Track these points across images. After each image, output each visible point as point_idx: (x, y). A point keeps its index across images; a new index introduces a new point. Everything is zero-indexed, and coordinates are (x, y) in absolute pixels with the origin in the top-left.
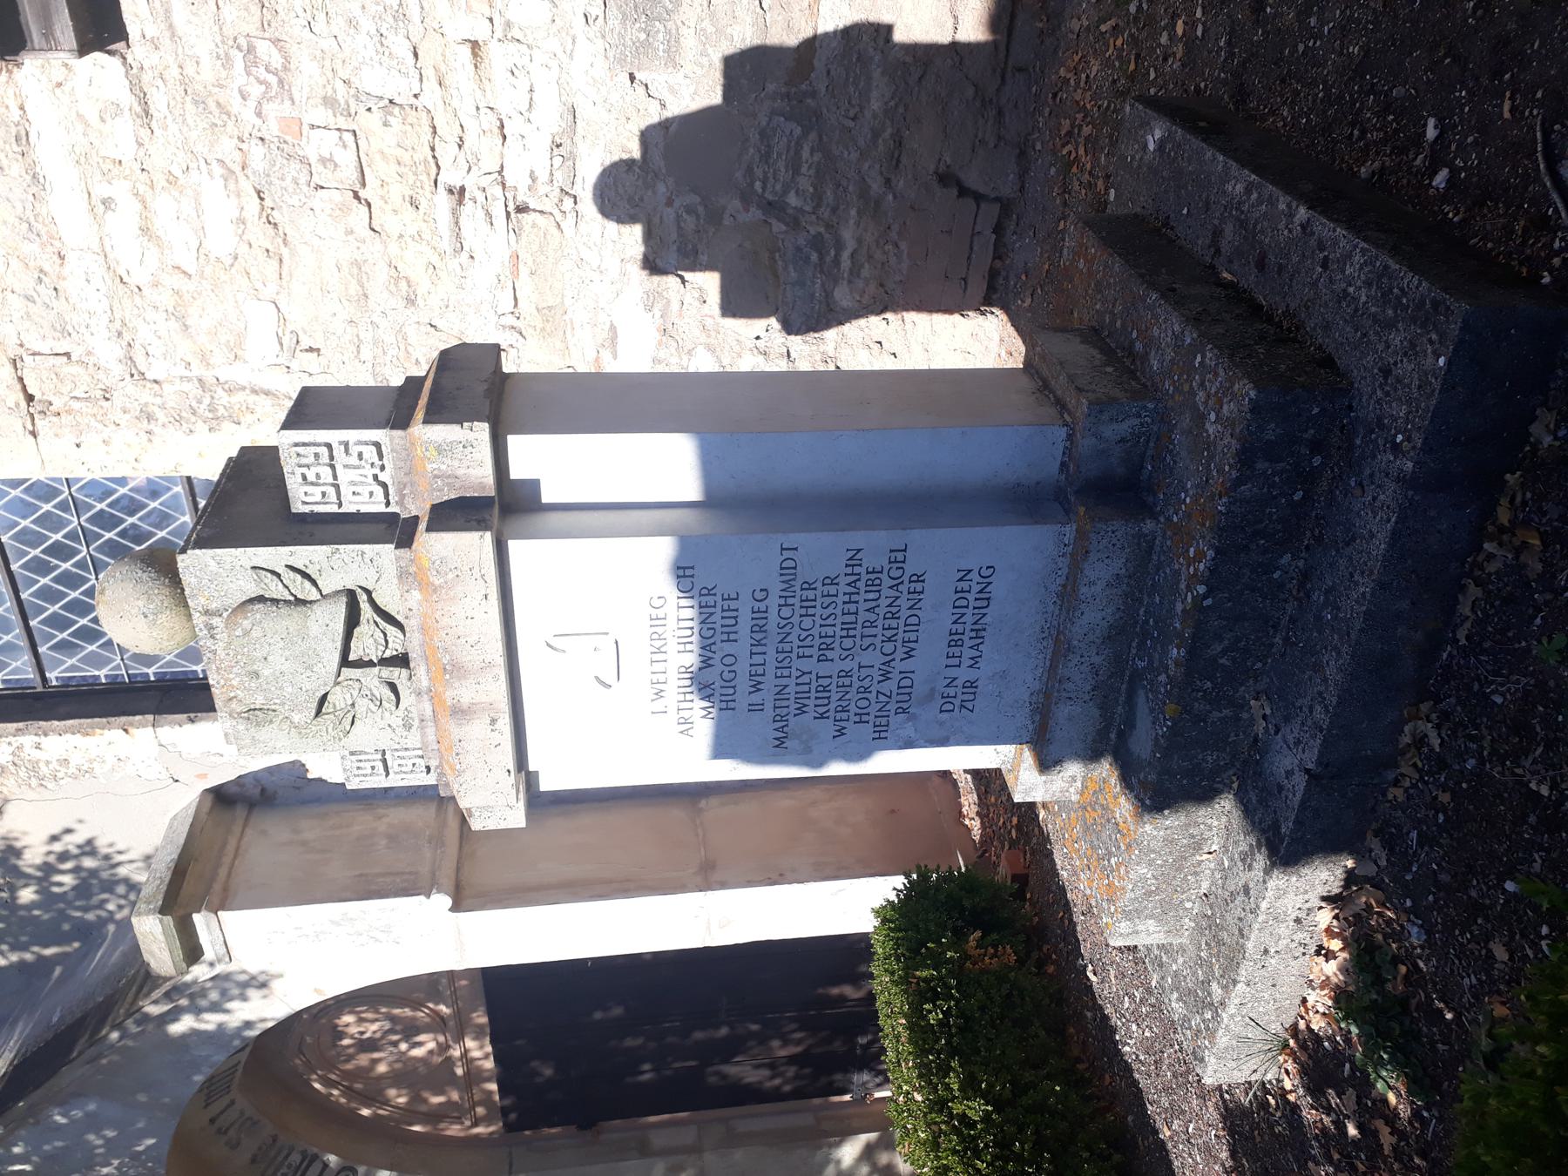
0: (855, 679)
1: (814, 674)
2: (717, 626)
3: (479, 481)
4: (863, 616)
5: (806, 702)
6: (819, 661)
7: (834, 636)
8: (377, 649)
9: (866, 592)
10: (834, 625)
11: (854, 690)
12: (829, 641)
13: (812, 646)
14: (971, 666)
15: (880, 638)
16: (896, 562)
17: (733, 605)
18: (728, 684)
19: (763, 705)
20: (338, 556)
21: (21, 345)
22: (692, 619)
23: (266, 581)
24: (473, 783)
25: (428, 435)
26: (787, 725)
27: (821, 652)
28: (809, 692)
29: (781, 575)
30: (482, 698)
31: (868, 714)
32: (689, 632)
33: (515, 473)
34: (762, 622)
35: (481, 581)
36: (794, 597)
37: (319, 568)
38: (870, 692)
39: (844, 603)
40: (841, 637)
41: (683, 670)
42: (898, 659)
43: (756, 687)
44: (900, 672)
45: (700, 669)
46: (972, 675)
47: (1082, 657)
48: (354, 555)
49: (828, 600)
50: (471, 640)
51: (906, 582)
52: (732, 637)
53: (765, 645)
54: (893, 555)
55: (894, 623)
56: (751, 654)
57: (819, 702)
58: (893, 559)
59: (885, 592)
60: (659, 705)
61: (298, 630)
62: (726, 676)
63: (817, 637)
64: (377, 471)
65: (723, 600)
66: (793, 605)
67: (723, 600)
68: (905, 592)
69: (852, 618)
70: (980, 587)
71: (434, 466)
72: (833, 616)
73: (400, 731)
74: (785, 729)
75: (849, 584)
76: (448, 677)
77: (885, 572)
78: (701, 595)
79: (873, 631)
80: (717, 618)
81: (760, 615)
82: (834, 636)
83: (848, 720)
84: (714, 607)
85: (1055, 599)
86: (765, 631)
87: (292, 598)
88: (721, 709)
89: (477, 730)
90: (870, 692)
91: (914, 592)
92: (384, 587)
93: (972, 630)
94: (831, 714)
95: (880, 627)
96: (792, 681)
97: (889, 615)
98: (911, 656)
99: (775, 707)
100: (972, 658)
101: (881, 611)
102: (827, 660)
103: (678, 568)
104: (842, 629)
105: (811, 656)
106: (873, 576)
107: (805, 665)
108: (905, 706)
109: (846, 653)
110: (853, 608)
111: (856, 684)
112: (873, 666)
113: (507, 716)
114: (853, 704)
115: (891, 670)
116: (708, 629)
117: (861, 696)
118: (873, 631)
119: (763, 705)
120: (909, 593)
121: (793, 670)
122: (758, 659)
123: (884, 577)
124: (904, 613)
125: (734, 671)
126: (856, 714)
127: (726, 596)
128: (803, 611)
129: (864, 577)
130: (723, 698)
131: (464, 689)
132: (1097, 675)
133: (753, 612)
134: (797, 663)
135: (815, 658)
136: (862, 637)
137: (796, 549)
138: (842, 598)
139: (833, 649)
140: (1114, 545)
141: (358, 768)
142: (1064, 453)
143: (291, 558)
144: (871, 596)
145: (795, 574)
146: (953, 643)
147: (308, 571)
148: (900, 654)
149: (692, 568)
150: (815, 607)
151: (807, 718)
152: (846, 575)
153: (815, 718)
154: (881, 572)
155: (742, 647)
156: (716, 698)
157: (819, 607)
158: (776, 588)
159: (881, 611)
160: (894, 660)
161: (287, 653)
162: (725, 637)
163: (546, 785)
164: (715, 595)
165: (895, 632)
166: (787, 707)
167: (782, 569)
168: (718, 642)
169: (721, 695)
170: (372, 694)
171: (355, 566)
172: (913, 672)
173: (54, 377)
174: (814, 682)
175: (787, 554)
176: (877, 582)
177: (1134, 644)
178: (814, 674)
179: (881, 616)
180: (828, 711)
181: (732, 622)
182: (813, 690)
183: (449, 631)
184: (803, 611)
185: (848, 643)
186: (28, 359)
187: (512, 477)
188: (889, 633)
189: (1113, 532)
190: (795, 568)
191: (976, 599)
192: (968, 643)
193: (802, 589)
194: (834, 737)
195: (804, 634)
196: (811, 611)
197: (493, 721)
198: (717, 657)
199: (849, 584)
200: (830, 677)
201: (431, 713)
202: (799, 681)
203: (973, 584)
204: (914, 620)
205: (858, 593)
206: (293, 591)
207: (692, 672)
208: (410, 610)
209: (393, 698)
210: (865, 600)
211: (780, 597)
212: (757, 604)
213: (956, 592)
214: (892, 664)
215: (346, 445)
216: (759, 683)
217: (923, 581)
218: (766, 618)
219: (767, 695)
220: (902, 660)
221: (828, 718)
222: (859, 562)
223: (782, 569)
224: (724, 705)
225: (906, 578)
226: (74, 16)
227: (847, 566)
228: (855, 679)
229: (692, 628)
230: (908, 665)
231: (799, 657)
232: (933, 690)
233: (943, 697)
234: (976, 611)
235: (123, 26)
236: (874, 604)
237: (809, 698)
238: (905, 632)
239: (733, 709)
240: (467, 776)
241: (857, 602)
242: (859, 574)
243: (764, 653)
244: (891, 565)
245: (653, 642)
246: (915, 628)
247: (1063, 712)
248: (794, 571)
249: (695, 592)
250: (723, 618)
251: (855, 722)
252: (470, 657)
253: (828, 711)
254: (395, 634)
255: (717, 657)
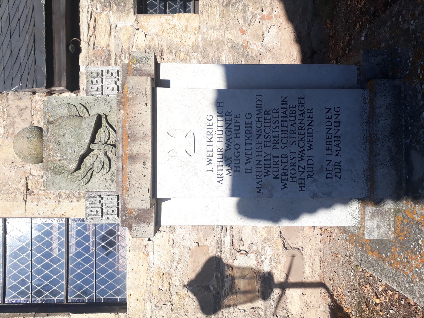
0: (289, 159)
1: (271, 155)
2: (232, 130)
3: (149, 72)
4: (290, 128)
5: (269, 169)
6: (273, 149)
7: (278, 137)
8: (105, 138)
9: (290, 116)
10: (278, 132)
11: (288, 164)
12: (277, 139)
13: (270, 141)
14: (336, 155)
15: (297, 139)
16: (301, 103)
17: (238, 120)
18: (237, 159)
19: (251, 169)
20: (97, 100)
21: (30, 173)
22: (222, 126)
23: (71, 108)
24: (133, 195)
25: (134, 54)
26: (261, 181)
27: (274, 144)
28: (270, 164)
29: (256, 107)
30: (142, 151)
31: (296, 177)
32: (221, 132)
33: (162, 78)
34: (249, 129)
35: (145, 97)
36: (262, 117)
37: (90, 105)
38: (295, 166)
39: (282, 121)
40: (282, 137)
41: (219, 150)
42: (306, 150)
43: (248, 161)
44: (308, 157)
45: (226, 150)
46: (337, 159)
47: (383, 143)
48: (103, 100)
49: (275, 120)
50: (140, 123)
51: (306, 112)
52: (238, 135)
53: (251, 140)
54: (300, 100)
55: (302, 132)
56: (246, 144)
57: (275, 170)
58: (299, 102)
59: (298, 117)
60: (209, 168)
61: (78, 125)
62: (237, 154)
63: (272, 137)
64: (116, 80)
65: (234, 118)
66: (261, 121)
67: (234, 118)
68: (306, 117)
69: (285, 129)
70: (335, 117)
71: (135, 66)
72: (278, 127)
73: (109, 182)
74: (261, 183)
75: (283, 113)
76: (129, 140)
77: (297, 107)
78: (226, 115)
79: (294, 135)
80: (232, 126)
81: (248, 125)
82: (278, 137)
83: (287, 180)
84: (231, 121)
85: (366, 124)
86: (251, 133)
87: (78, 115)
88: (234, 171)
89: (138, 166)
90: (295, 166)
91: (309, 118)
92: (112, 114)
93: (335, 137)
94: (280, 176)
95: (297, 133)
96: (262, 158)
97: (300, 128)
98: (311, 149)
99: (256, 171)
100: (337, 151)
101: (297, 125)
102: (276, 149)
103: (218, 102)
104: (282, 134)
105: (270, 146)
106: (292, 109)
107: (268, 150)
108: (311, 174)
109: (284, 146)
110: (285, 123)
111: (290, 161)
112: (295, 153)
113: (150, 161)
114: (289, 172)
115: (303, 155)
116: (229, 131)
117: (292, 167)
118: (294, 135)
119: (251, 169)
120: (307, 118)
121: (263, 153)
122: (248, 147)
123: (297, 109)
124: (306, 127)
125: (239, 152)
126: (291, 177)
127: (235, 116)
128: (266, 124)
129: (289, 110)
130: (235, 165)
131: (134, 147)
132: (391, 152)
133: (246, 124)
134: (264, 150)
135: (272, 147)
136: (290, 138)
137: (262, 96)
138: (281, 119)
139: (278, 143)
140: (385, 90)
141: (91, 211)
142: (358, 76)
143: (81, 101)
144: (292, 118)
145: (261, 107)
146: (328, 143)
147: (86, 106)
148: (306, 148)
149: (223, 103)
150: (270, 122)
151: (270, 177)
152: (282, 108)
153: (273, 178)
154: (295, 108)
155: (242, 141)
156: (232, 165)
157: (272, 122)
158: (254, 113)
159: (297, 125)
160: (304, 150)
161: (72, 134)
162: (235, 135)
163: (163, 204)
164: (231, 115)
165: (303, 136)
166: (261, 171)
167: (257, 104)
168: (233, 138)
169: (234, 164)
170: (101, 160)
171: (103, 105)
172: (313, 157)
173: (36, 182)
174: (272, 159)
175: (258, 98)
176: (294, 112)
177: (403, 137)
178: (271, 155)
179: (297, 128)
180: (278, 175)
181: (238, 128)
182: (272, 164)
183: (132, 119)
184: (266, 124)
185: (284, 140)
186: (31, 177)
187: (161, 79)
188: (301, 137)
189: (384, 84)
190: (261, 104)
191: (335, 122)
192: (335, 143)
193: (265, 114)
194: (282, 189)
195: (267, 135)
196: (269, 124)
197: (145, 163)
198: (232, 145)
199: (283, 113)
200: (278, 157)
201: (122, 168)
202: (266, 158)
203: (333, 115)
204: (310, 131)
205: (287, 117)
206: (79, 112)
207: (222, 152)
208: (119, 118)
209: (108, 163)
210: (290, 120)
211: (256, 117)
212: (247, 120)
213: (326, 118)
214: (304, 152)
215: (108, 71)
216: (250, 159)
217: (312, 112)
218: (251, 127)
219: (252, 165)
220: (308, 150)
221: (279, 178)
222: (286, 103)
223: (257, 104)
224: (235, 169)
225: (305, 111)
226: (67, 78)
227: (282, 104)
228: (289, 159)
229: (222, 131)
230: (310, 153)
231: (265, 146)
232: (322, 166)
233: (327, 171)
234: (335, 128)
235: (79, 86)
236: (293, 122)
237: (270, 167)
238: (307, 136)
239: (239, 171)
240: (132, 191)
241: (287, 121)
242: (287, 108)
243: (251, 144)
244: (299, 104)
245: (208, 136)
246: (311, 135)
247: (380, 171)
248: (260, 106)
249: (224, 114)
250: (234, 126)
251: (291, 181)
252: (139, 132)
253: (278, 175)
254: (113, 133)
255: (232, 145)
